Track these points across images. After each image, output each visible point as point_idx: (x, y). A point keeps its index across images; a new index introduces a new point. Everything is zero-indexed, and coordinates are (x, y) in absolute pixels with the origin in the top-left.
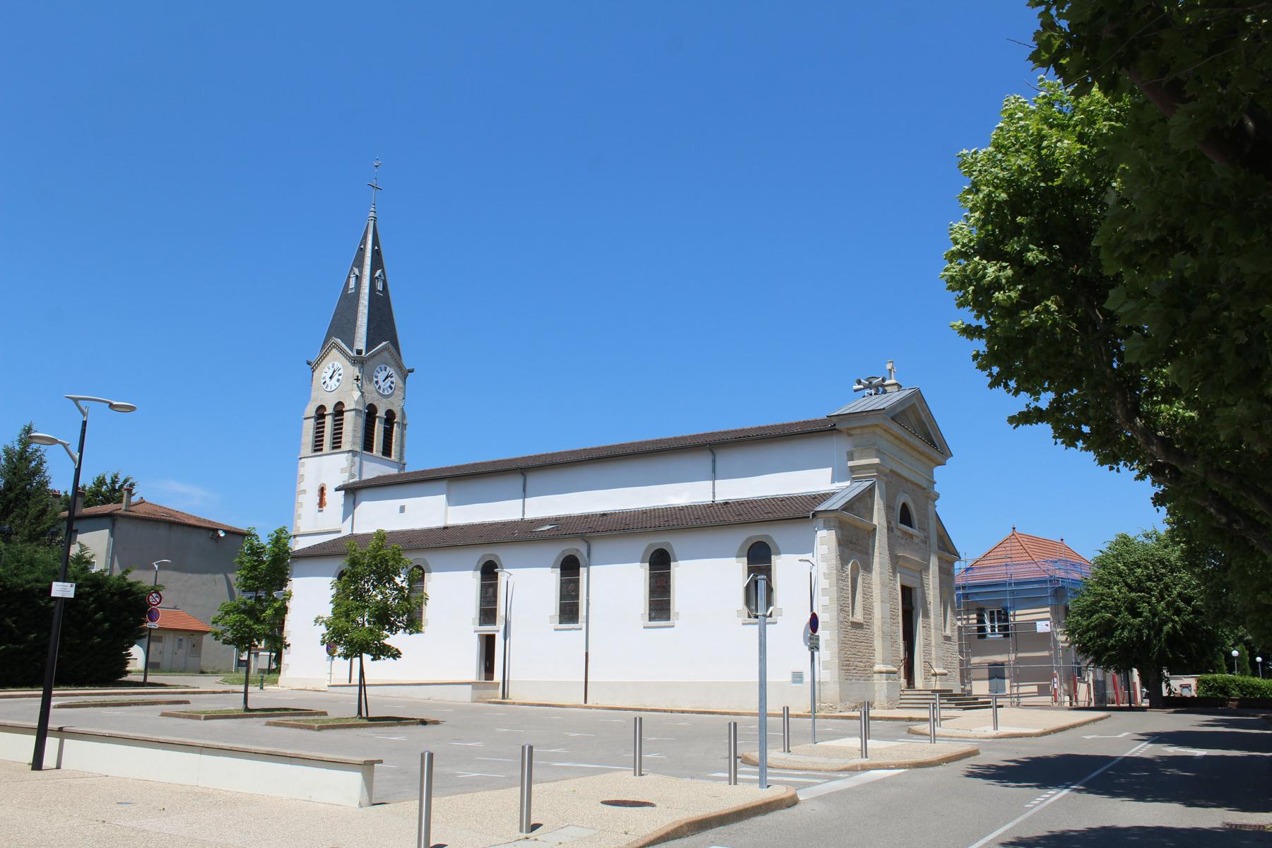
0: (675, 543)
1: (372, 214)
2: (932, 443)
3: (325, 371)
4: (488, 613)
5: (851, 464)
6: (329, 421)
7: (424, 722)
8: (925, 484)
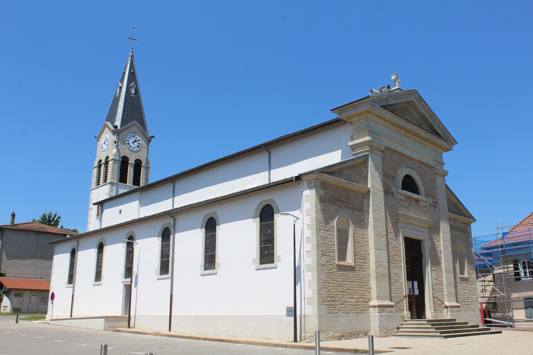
1: (131, 53)
2: (437, 134)
3: (102, 140)
8: (431, 163)
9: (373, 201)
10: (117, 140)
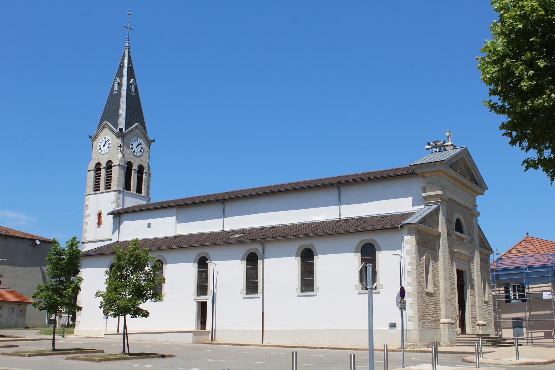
0: (316, 244)
1: (127, 45)
2: (475, 182)
3: (100, 141)
4: (202, 289)
5: (424, 194)
6: (103, 172)
7: (163, 356)
8: (470, 206)
9: (443, 242)
10: (122, 144)
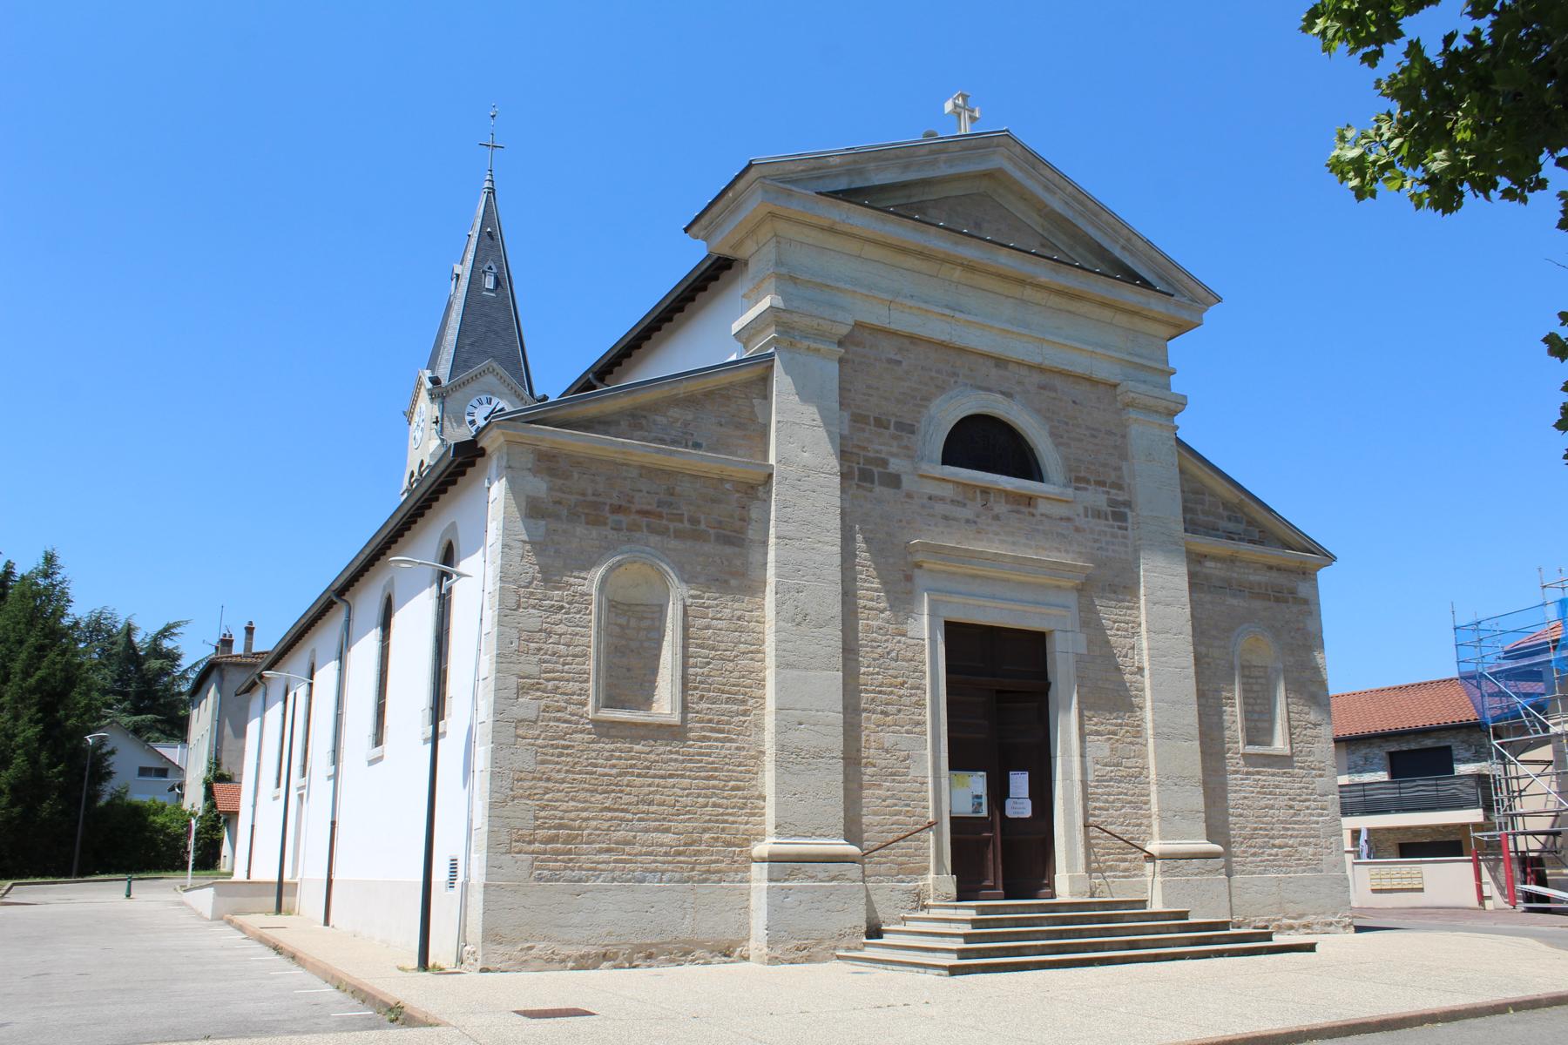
2: (1132, 277)
9: (783, 506)
